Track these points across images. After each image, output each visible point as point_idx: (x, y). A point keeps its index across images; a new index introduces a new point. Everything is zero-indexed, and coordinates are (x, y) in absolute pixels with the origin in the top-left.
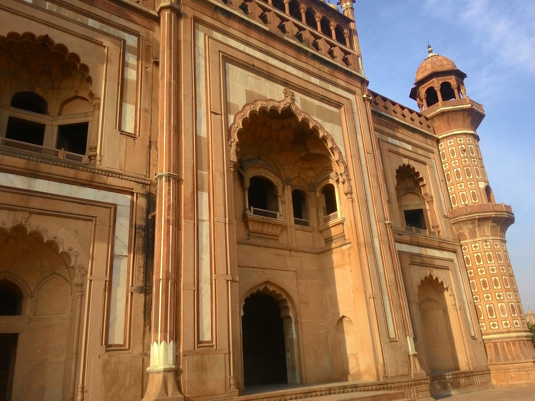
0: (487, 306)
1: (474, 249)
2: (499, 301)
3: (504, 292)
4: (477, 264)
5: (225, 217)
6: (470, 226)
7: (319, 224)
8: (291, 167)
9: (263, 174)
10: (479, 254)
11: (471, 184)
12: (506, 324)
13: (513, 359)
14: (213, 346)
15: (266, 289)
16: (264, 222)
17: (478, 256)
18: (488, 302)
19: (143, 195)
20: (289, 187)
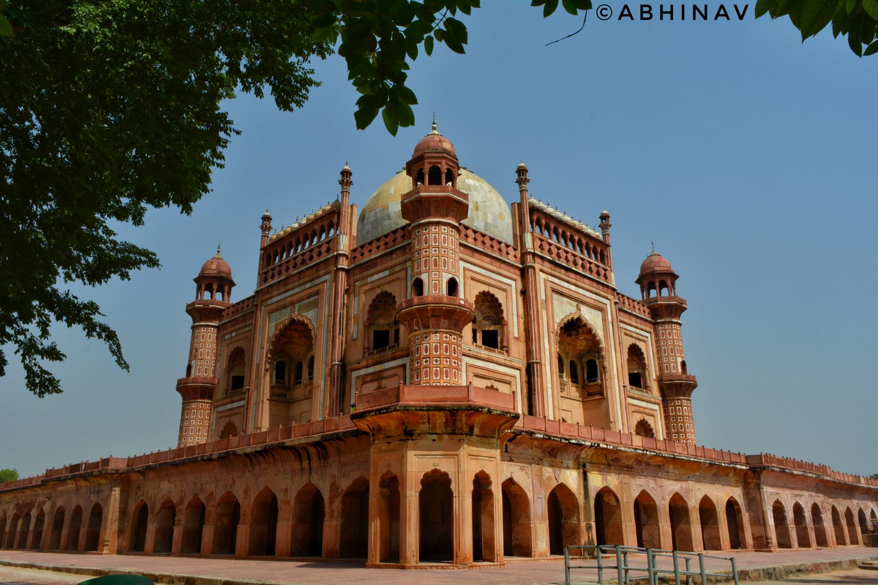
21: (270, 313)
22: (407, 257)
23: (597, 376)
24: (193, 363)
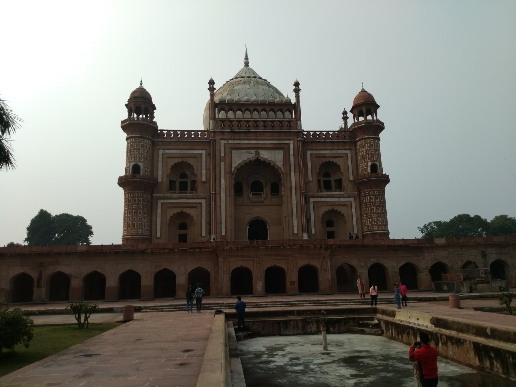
21: (232, 149)
22: (348, 147)
24: (141, 164)
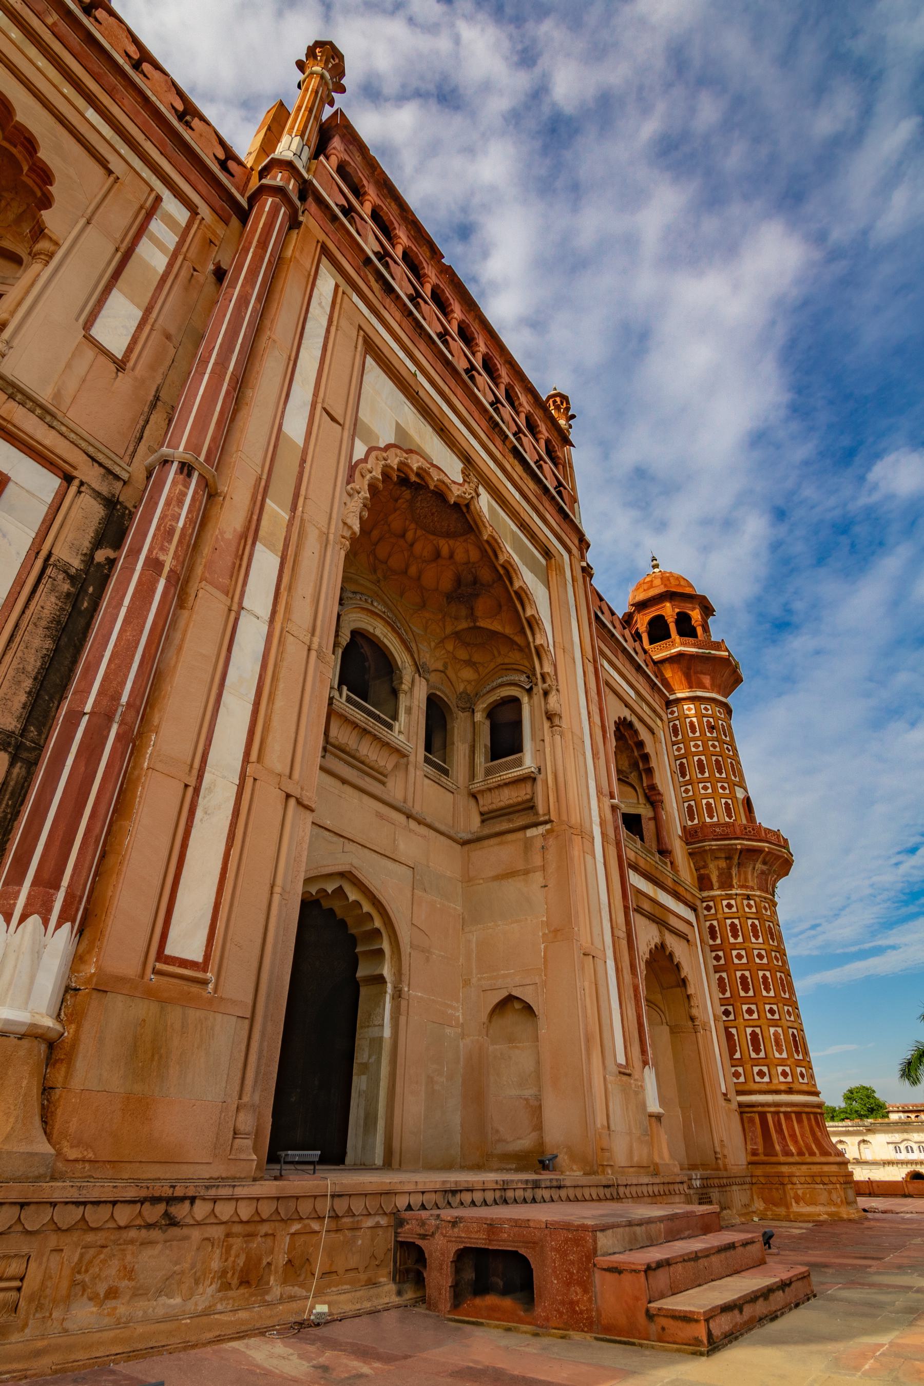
0: (749, 1030)
1: (726, 910)
2: (771, 1023)
3: (780, 1005)
4: (732, 940)
5: (313, 635)
6: (723, 864)
7: (472, 776)
8: (433, 644)
9: (378, 632)
10: (736, 921)
11: (723, 788)
12: (784, 1074)
13: (801, 1153)
14: (205, 983)
15: (340, 891)
16: (365, 730)
17: (733, 925)
18: (751, 1023)
19: (97, 494)
20: (424, 682)
23: (519, 749)
